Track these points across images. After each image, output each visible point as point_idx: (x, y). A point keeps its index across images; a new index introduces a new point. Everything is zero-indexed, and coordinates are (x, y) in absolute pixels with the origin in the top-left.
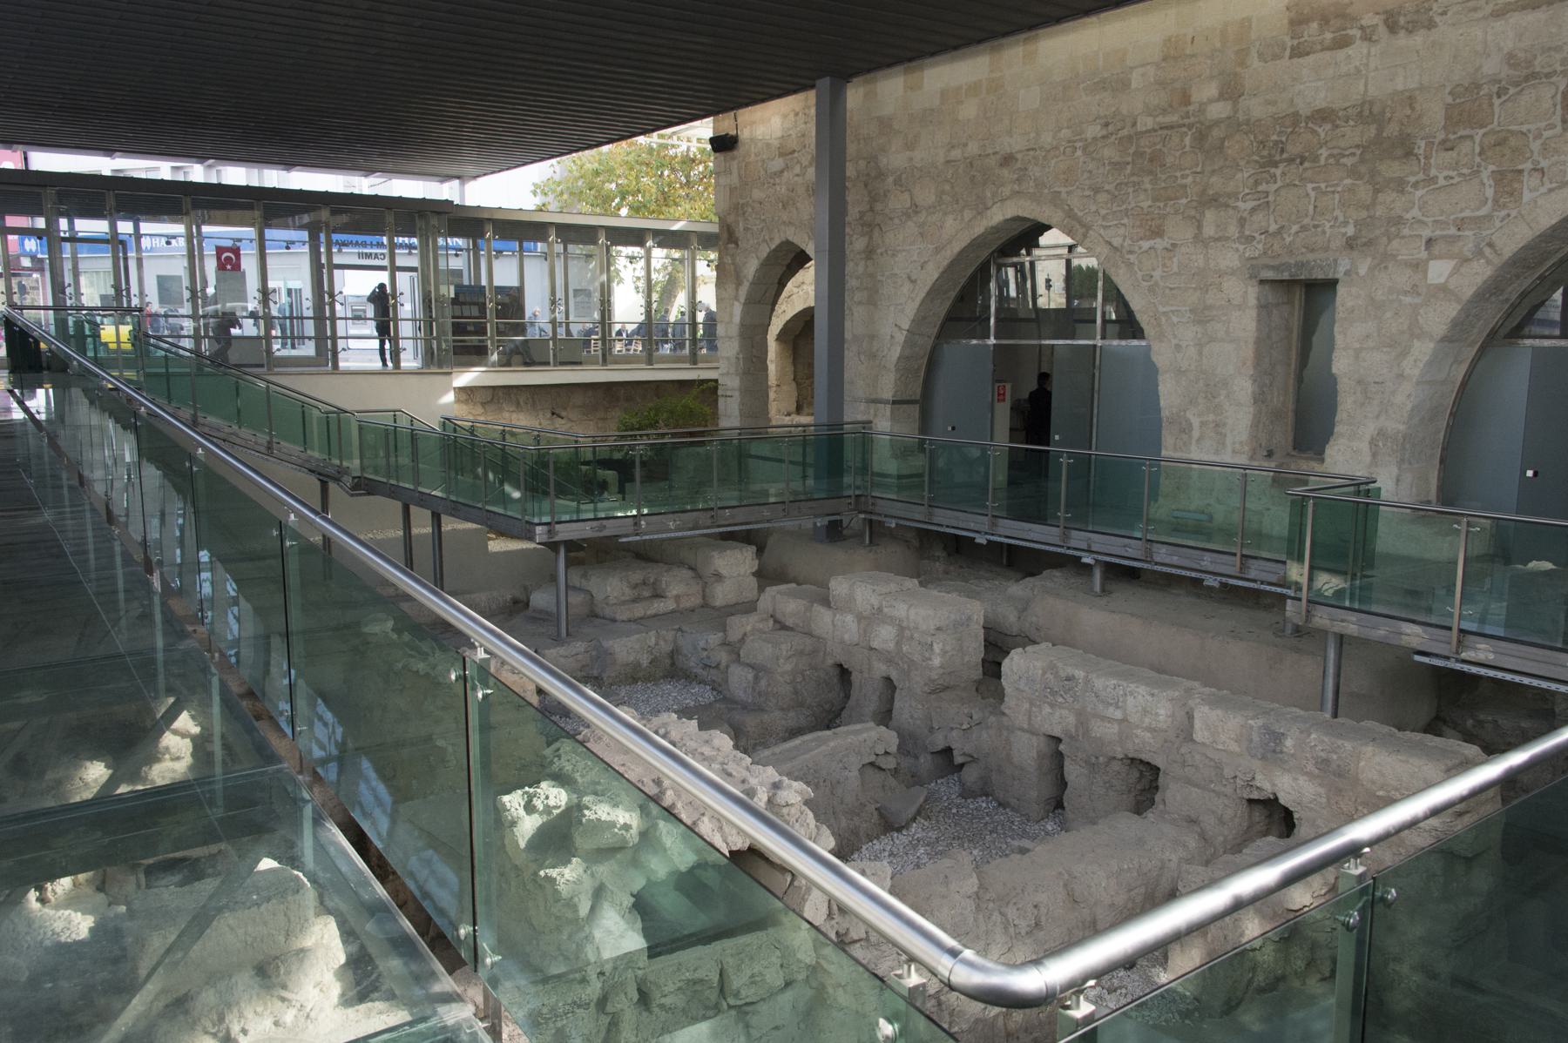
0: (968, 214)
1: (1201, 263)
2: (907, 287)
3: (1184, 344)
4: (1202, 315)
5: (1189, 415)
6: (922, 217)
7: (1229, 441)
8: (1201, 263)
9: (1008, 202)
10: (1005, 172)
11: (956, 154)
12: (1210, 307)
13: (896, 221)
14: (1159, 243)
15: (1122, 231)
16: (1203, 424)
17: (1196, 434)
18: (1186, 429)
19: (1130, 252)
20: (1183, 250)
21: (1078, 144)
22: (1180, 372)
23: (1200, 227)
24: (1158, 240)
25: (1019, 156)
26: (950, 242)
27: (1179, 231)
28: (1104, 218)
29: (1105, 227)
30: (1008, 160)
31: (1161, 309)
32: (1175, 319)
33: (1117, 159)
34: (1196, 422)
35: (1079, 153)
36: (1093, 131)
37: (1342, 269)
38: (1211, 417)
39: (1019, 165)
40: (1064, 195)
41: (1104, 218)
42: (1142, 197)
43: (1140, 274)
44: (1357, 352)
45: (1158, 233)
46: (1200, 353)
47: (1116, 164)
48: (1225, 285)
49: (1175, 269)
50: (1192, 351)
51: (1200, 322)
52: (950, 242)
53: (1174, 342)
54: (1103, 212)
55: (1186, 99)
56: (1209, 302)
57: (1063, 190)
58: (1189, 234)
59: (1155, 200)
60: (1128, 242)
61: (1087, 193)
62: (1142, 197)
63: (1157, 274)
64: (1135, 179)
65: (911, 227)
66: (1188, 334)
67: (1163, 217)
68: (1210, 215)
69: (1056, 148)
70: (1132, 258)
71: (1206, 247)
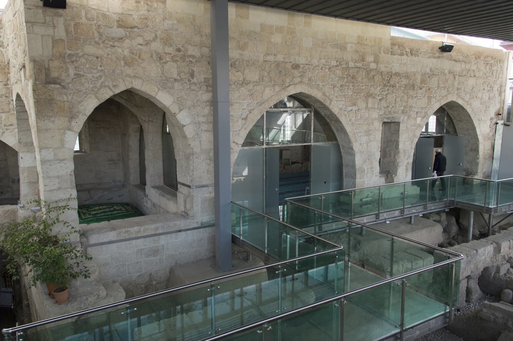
0: (277, 89)
1: (367, 116)
2: (240, 122)
3: (362, 143)
4: (368, 133)
5: (364, 166)
6: (250, 87)
7: (374, 173)
8: (367, 116)
9: (298, 86)
10: (296, 72)
11: (271, 58)
12: (370, 130)
13: (233, 86)
14: (354, 108)
15: (343, 103)
16: (368, 168)
17: (366, 172)
18: (363, 172)
19: (345, 111)
20: (362, 111)
21: (327, 67)
22: (362, 152)
23: (367, 104)
24: (354, 107)
25: (301, 66)
26: (267, 100)
27: (362, 104)
28: (336, 97)
29: (337, 101)
30: (296, 67)
31: (356, 131)
32: (360, 135)
33: (341, 75)
34: (366, 168)
35: (327, 70)
36: (334, 63)
37: (401, 119)
38: (370, 166)
39: (301, 70)
40: (321, 86)
41: (336, 97)
42: (350, 91)
43: (348, 119)
44: (404, 142)
45: (354, 104)
46: (367, 146)
47: (341, 77)
48: (374, 123)
49: (359, 117)
50: (365, 145)
51: (367, 135)
52: (267, 100)
53: (360, 142)
54: (336, 95)
55: (363, 60)
56: (370, 129)
57: (321, 84)
58: (364, 106)
59: (354, 92)
60: (344, 107)
61: (331, 87)
62: (350, 91)
63: (353, 119)
64: (347, 84)
65: (244, 91)
66: (364, 139)
67: (357, 99)
68: (370, 100)
69: (318, 66)
70: (346, 113)
71: (369, 110)
